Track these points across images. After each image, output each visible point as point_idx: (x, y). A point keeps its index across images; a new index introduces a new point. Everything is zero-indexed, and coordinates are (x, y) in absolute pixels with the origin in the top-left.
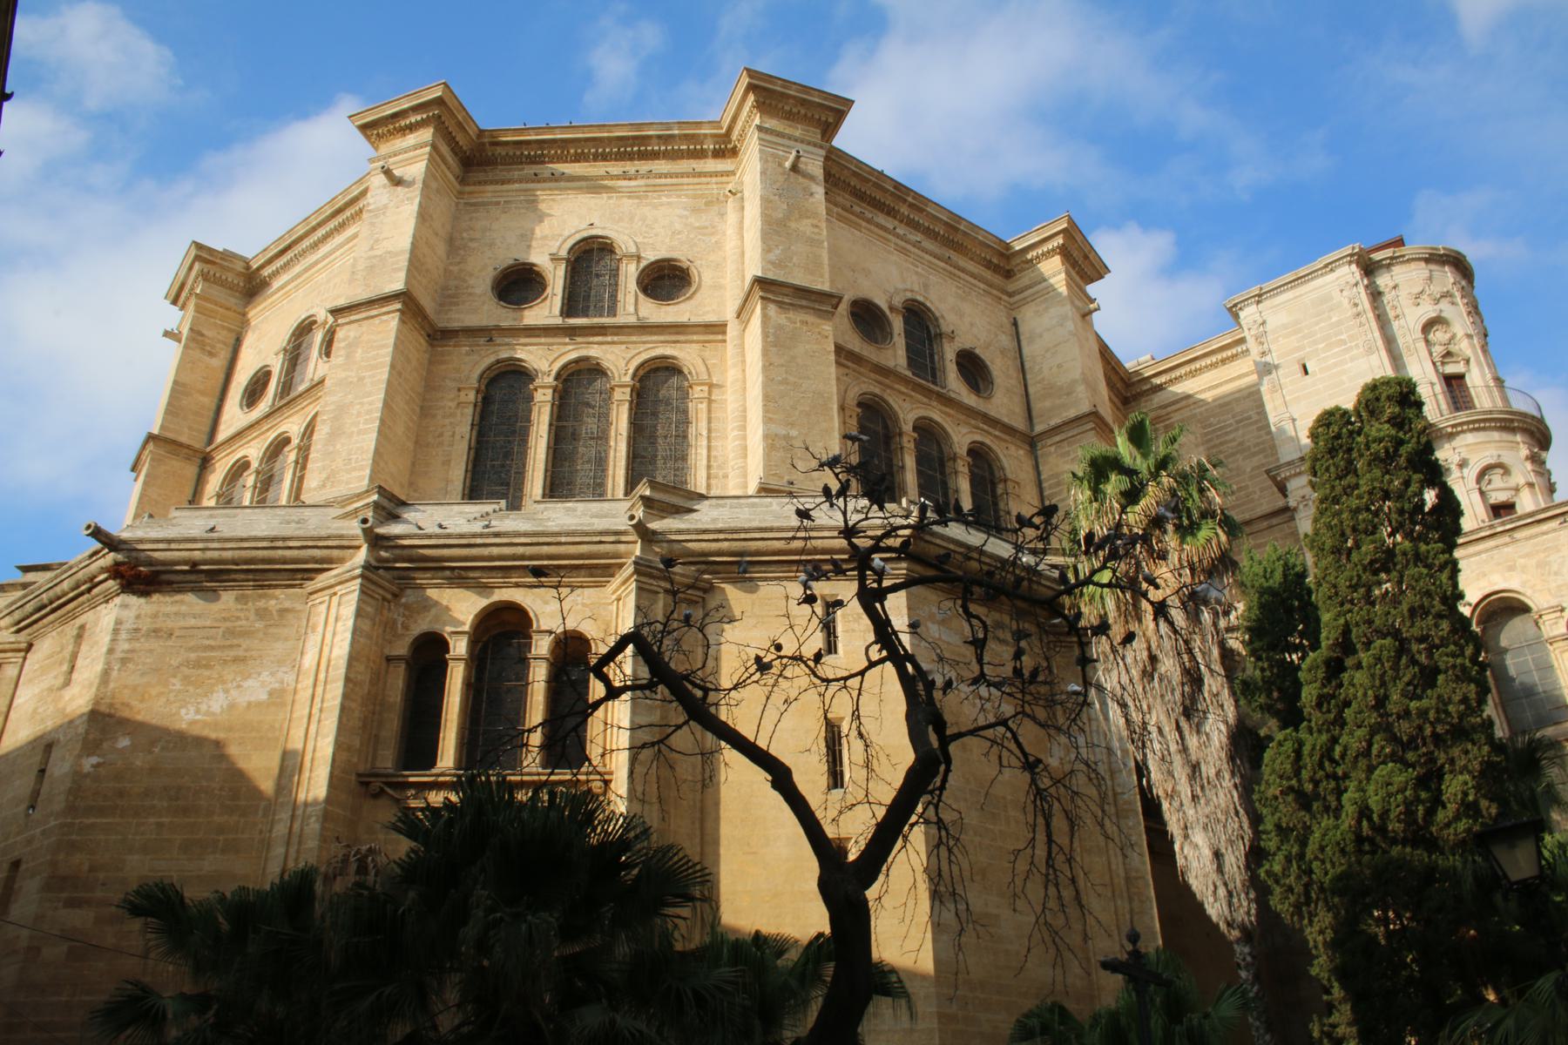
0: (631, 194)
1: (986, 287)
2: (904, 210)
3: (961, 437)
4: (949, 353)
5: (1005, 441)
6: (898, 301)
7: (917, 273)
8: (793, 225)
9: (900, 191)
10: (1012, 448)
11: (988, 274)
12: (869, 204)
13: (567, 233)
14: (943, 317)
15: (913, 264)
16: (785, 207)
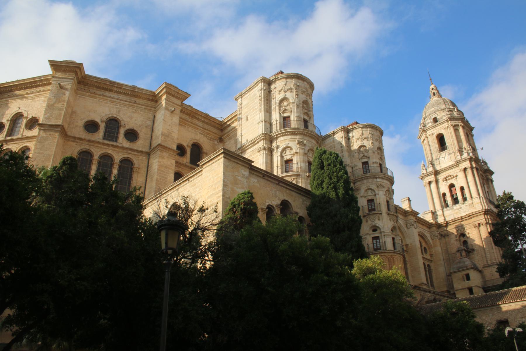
0: (31, 99)
1: (146, 107)
2: (115, 89)
3: (118, 157)
4: (122, 131)
5: (138, 155)
6: (105, 119)
7: (117, 108)
8: (56, 105)
9: (113, 83)
10: (141, 157)
11: (149, 103)
12: (102, 89)
13: (13, 112)
14: (123, 120)
15: (116, 105)
16: (55, 100)
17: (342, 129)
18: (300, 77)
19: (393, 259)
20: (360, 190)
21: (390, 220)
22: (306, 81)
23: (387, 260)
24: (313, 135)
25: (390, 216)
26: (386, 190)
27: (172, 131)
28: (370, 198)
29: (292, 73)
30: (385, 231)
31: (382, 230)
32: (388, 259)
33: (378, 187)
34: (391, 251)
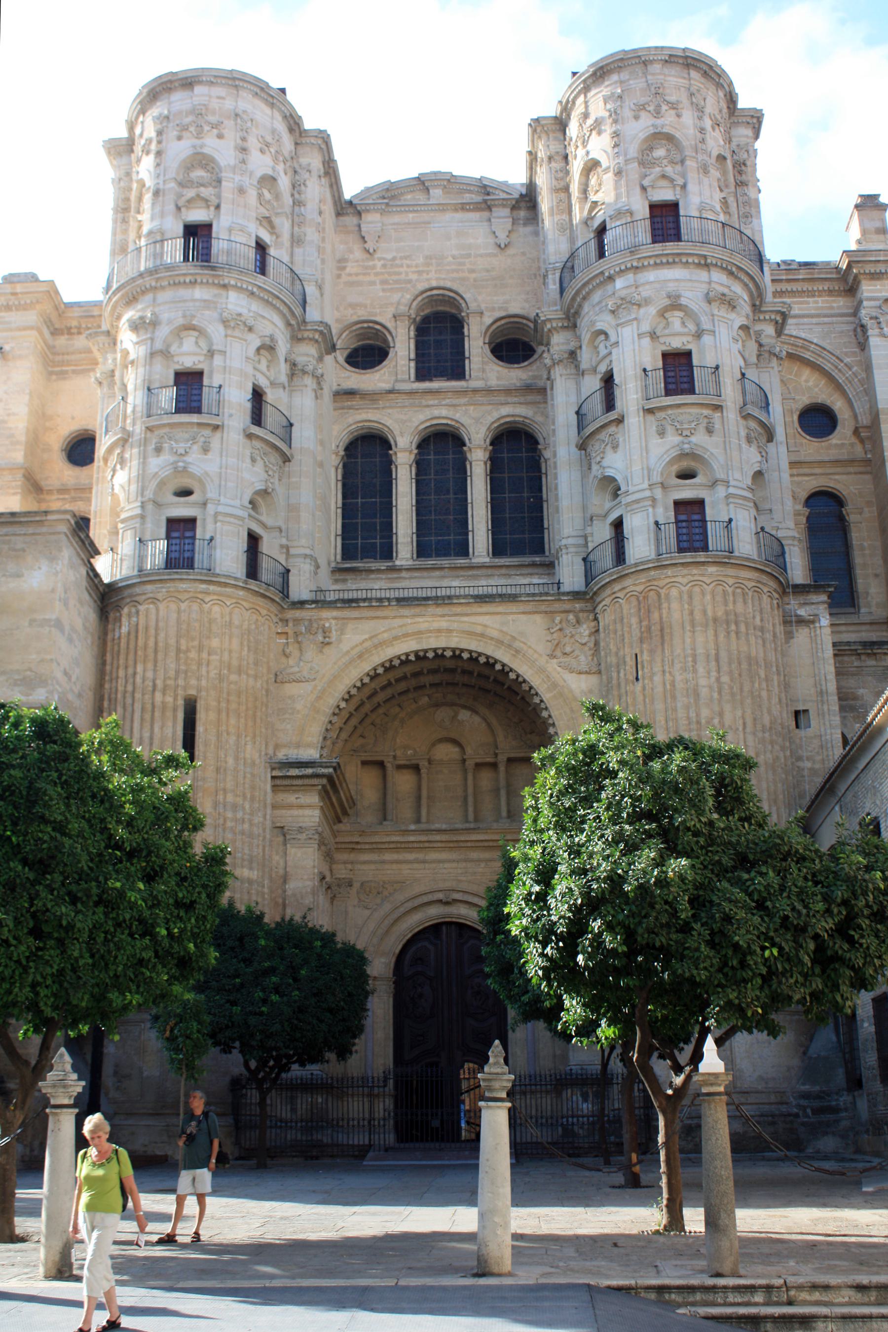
17: (534, 131)
18: (171, 82)
19: (659, 595)
20: (580, 347)
21: (662, 433)
22: (200, 82)
23: (634, 602)
24: (185, 275)
25: (661, 415)
26: (652, 310)
27: (9, 415)
28: (603, 368)
29: (143, 87)
30: (631, 489)
31: (623, 489)
32: (638, 599)
33: (613, 312)
34: (642, 563)
